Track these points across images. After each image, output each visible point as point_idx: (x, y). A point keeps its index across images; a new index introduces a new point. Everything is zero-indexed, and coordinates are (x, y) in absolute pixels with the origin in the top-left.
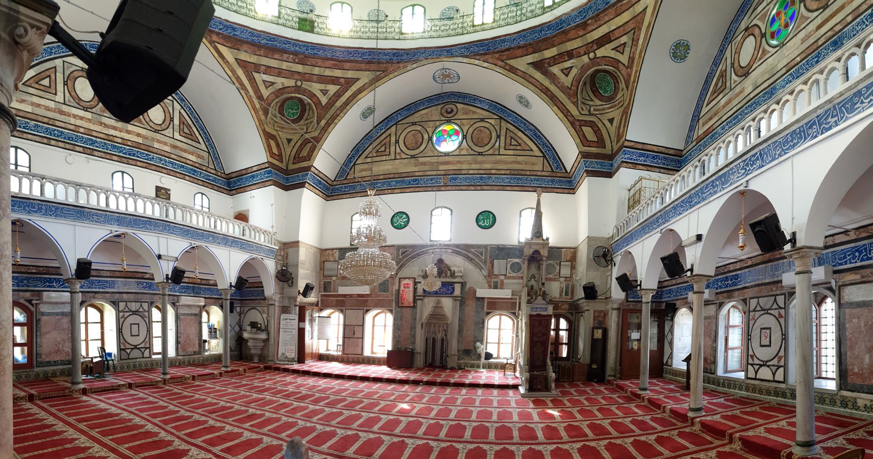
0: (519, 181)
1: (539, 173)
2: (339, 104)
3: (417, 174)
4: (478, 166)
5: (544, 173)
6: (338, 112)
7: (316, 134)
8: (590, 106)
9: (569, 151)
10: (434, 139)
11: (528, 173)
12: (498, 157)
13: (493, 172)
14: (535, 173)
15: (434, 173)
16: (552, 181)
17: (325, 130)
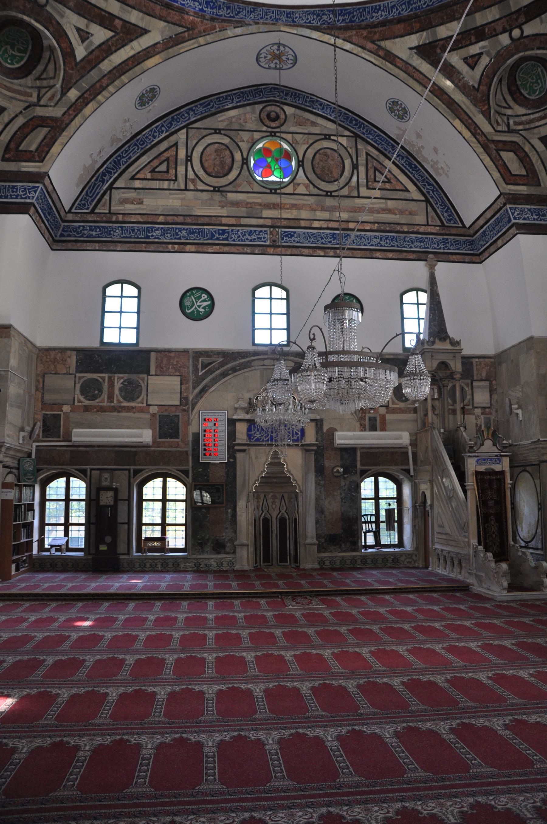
0: (392, 243)
1: (422, 229)
2: (106, 66)
3: (224, 221)
4: (326, 215)
5: (430, 229)
6: (105, 82)
7: (57, 112)
8: (508, 117)
9: (475, 189)
10: (252, 162)
11: (405, 229)
12: (357, 201)
13: (351, 225)
14: (416, 229)
15: (254, 221)
16: (445, 242)
17: (77, 108)
